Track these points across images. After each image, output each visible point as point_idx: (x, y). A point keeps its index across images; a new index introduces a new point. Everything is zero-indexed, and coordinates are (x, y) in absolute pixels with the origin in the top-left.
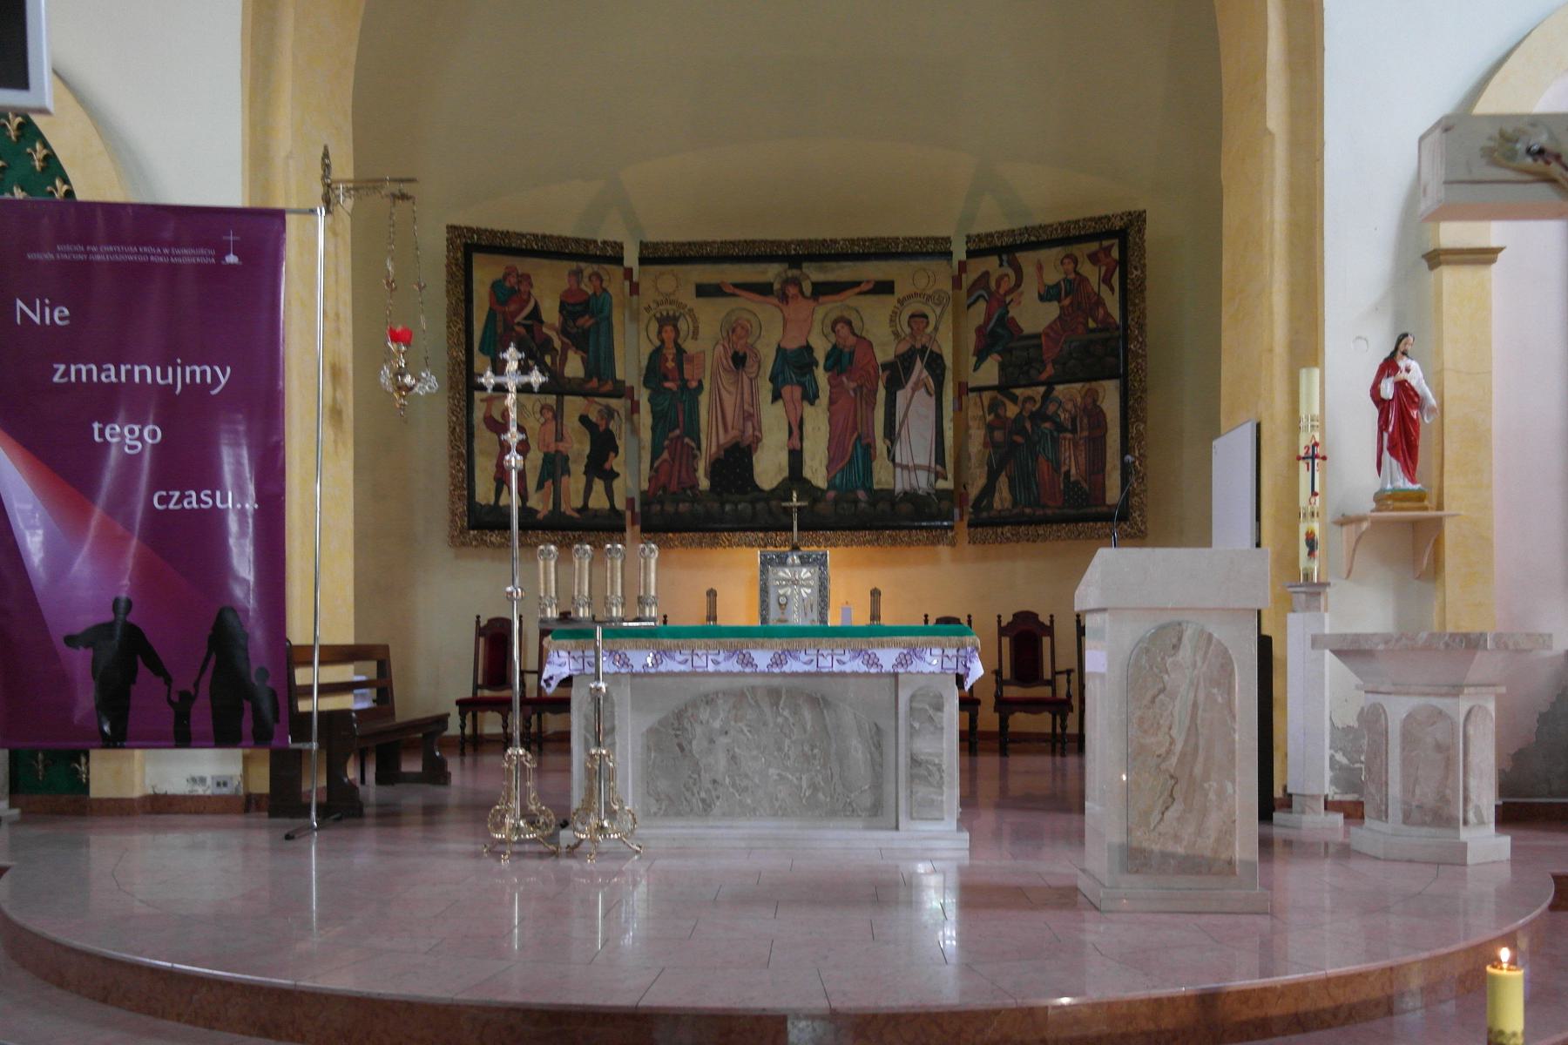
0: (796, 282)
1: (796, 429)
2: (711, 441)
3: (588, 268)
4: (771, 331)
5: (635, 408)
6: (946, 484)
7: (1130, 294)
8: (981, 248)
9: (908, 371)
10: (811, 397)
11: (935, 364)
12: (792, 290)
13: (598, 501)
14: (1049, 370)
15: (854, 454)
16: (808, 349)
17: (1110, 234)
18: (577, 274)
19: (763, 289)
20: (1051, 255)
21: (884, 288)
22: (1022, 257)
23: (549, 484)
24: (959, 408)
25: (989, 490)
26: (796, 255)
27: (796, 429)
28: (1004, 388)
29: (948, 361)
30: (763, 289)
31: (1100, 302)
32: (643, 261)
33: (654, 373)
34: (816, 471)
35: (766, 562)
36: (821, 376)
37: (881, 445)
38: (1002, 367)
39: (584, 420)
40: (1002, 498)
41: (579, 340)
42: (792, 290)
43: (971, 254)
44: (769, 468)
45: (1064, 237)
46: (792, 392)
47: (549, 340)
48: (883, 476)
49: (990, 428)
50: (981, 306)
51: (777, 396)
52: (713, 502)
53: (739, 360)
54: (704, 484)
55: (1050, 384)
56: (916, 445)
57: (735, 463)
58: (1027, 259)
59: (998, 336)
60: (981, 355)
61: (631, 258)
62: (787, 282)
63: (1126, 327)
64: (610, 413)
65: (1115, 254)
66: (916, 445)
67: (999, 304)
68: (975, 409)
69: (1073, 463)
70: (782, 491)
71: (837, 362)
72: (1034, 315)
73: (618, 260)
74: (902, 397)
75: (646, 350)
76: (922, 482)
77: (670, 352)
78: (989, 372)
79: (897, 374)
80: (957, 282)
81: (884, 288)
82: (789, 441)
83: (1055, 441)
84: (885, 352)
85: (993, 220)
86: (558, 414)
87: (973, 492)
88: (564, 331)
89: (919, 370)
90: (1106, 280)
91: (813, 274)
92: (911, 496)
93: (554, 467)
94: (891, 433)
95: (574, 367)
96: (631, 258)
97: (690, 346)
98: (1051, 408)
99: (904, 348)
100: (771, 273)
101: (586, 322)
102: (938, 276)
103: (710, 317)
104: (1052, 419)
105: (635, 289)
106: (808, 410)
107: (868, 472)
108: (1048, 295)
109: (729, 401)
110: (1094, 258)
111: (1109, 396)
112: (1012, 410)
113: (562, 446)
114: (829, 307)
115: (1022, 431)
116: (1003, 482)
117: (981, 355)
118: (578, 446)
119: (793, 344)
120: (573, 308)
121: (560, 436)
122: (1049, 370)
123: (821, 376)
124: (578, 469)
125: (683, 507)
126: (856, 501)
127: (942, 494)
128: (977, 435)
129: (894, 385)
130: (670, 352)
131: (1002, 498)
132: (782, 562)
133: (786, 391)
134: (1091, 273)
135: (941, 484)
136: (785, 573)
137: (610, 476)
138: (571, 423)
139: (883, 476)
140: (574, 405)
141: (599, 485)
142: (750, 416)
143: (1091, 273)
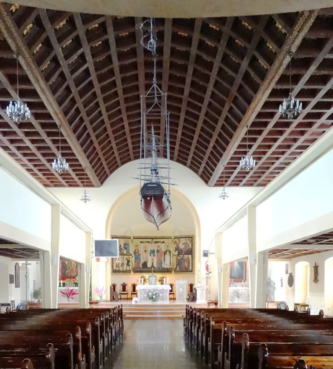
0: (153, 241)
1: (153, 260)
2: (142, 262)
3: (127, 239)
5: (132, 257)
7: (193, 245)
9: (166, 253)
10: (154, 256)
11: (170, 252)
12: (152, 242)
13: (128, 269)
14: (183, 253)
15: (160, 262)
16: (154, 250)
17: (191, 237)
19: (149, 242)
21: (163, 242)
22: (180, 239)
23: (122, 267)
24: (173, 257)
25: (176, 268)
27: (153, 260)
28: (178, 255)
30: (149, 242)
31: (189, 245)
33: (135, 253)
34: (155, 265)
36: (156, 253)
38: (178, 252)
39: (126, 259)
40: (178, 269)
41: (126, 249)
42: (152, 242)
44: (149, 265)
46: (152, 255)
47: (122, 249)
49: (176, 260)
50: (175, 245)
51: (150, 256)
52: (143, 268)
53: (146, 251)
54: (141, 267)
55: (183, 255)
57: (145, 264)
59: (177, 249)
60: (175, 251)
61: (132, 238)
62: (152, 241)
63: (192, 248)
64: (129, 257)
65: (191, 239)
68: (175, 257)
69: (186, 265)
70: (151, 268)
71: (158, 251)
72: (182, 246)
73: (130, 238)
74: (165, 256)
76: (168, 267)
77: (137, 250)
78: (176, 253)
79: (165, 253)
80: (172, 242)
81: (163, 242)
82: (152, 261)
83: (184, 262)
84: (164, 250)
85: (177, 234)
86: (123, 258)
87: (174, 268)
89: (168, 252)
90: (190, 243)
91: (155, 240)
92: (167, 268)
93: (123, 264)
94: (164, 260)
96: (132, 238)
97: (139, 249)
98: (184, 258)
99: (166, 250)
101: (126, 246)
102: (170, 240)
103: (142, 245)
104: (184, 259)
105: (132, 242)
107: (162, 266)
108: (183, 244)
109: (144, 256)
110: (188, 240)
112: (179, 258)
115: (180, 261)
116: (178, 267)
118: (126, 262)
119: (152, 249)
120: (125, 245)
121: (123, 261)
122: (183, 253)
123: (156, 253)
125: (139, 269)
126: (160, 269)
127: (171, 268)
128: (175, 261)
129: (165, 254)
130: (137, 250)
131: (178, 269)
132: (151, 276)
133: (151, 255)
135: (171, 267)
136: (151, 278)
137: (129, 265)
139: (163, 266)
140: (125, 257)
141: (128, 266)
143: (188, 242)
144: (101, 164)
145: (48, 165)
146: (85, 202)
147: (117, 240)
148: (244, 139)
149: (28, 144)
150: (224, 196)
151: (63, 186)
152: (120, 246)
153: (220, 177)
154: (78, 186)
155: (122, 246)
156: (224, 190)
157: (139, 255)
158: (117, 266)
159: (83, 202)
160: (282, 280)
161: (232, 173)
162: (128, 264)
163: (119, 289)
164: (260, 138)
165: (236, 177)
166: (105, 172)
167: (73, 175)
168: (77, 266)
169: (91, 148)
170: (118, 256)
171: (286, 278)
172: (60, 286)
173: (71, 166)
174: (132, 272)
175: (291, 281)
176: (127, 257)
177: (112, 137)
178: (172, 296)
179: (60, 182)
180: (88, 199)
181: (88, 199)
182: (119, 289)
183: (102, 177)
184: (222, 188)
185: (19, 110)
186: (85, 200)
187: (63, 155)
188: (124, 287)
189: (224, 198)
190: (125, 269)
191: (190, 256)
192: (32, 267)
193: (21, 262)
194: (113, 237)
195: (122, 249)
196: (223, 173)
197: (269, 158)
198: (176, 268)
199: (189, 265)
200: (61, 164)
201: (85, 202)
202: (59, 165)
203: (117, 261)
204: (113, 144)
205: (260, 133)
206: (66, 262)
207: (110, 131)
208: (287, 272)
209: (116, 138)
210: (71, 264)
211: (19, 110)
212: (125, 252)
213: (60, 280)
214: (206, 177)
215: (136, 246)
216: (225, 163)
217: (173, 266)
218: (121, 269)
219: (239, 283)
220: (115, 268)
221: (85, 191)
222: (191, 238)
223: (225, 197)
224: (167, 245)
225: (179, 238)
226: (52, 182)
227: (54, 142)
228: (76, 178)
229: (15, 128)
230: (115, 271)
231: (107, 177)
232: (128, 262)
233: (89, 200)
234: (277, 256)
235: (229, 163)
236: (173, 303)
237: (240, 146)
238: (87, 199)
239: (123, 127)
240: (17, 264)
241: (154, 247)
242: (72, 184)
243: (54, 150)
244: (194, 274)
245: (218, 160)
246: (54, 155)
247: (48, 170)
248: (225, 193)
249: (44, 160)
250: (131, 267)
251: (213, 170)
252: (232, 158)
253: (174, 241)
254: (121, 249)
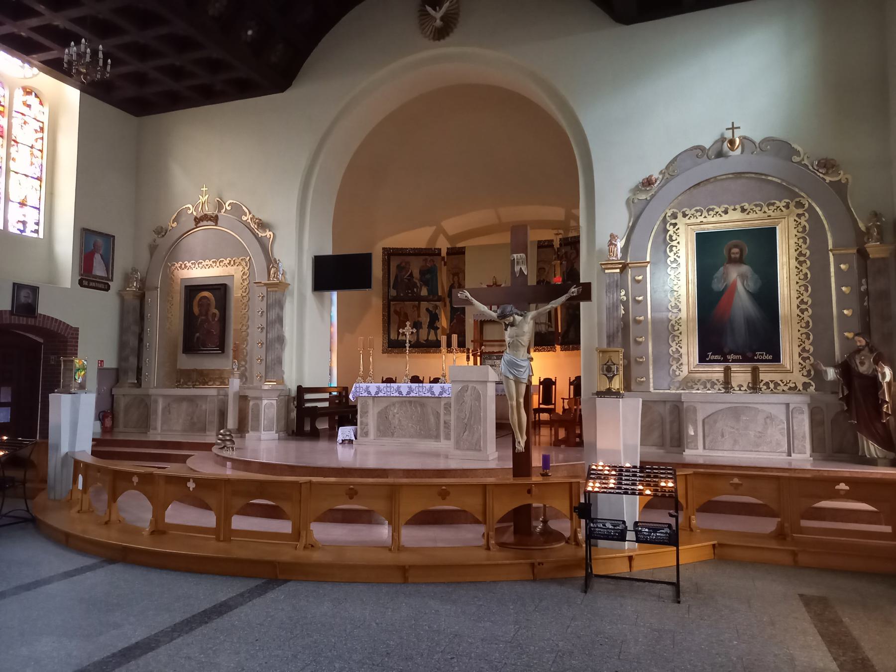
5: (445, 305)
6: (553, 329)
13: (432, 337)
18: (426, 260)
32: (448, 254)
39: (427, 310)
41: (426, 283)
64: (436, 307)
73: (439, 254)
86: (418, 307)
88: (421, 280)
95: (424, 292)
101: (428, 276)
113: (420, 319)
118: (425, 319)
120: (422, 273)
124: (425, 326)
135: (550, 329)
140: (424, 305)
141: (432, 332)
195: (415, 285)
212: (424, 292)
215: (454, 275)
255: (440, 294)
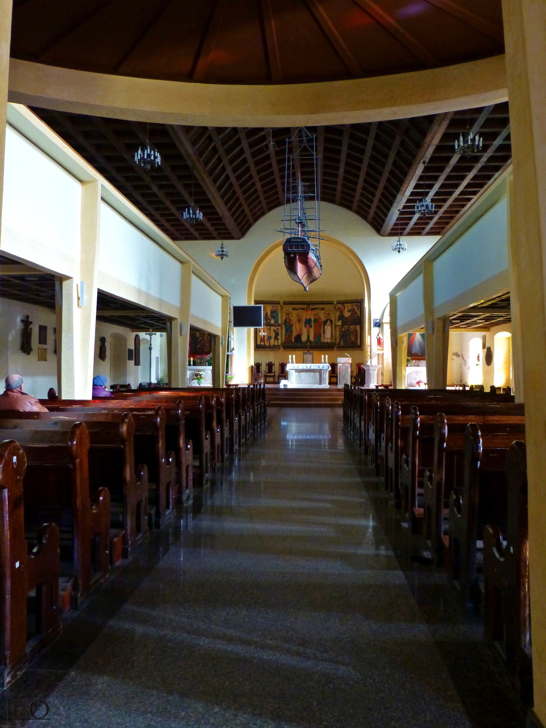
0: (309, 308)
1: (308, 332)
2: (295, 334)
4: (305, 315)
5: (282, 328)
8: (339, 302)
10: (311, 326)
11: (331, 322)
13: (276, 344)
15: (318, 335)
16: (310, 319)
19: (303, 309)
20: (349, 305)
24: (335, 328)
25: (340, 342)
26: (309, 304)
27: (308, 332)
28: (342, 326)
29: (333, 320)
30: (303, 309)
34: (312, 339)
35: (304, 354)
36: (313, 323)
37: (322, 335)
38: (342, 322)
39: (274, 330)
40: (342, 344)
41: (273, 317)
43: (337, 303)
44: (304, 338)
45: (352, 302)
48: (322, 340)
49: (340, 332)
51: (305, 326)
52: (294, 344)
54: (293, 341)
55: (349, 325)
56: (328, 335)
57: (299, 337)
58: (346, 305)
59: (341, 317)
60: (339, 320)
61: (282, 303)
62: (307, 308)
64: (278, 329)
66: (328, 335)
67: (342, 312)
68: (338, 329)
69: (353, 338)
70: (306, 342)
71: (316, 321)
72: (347, 314)
74: (326, 327)
75: (284, 319)
76: (329, 341)
78: (340, 323)
79: (325, 323)
80: (335, 308)
81: (323, 309)
84: (323, 319)
86: (270, 330)
90: (358, 309)
91: (312, 306)
92: (327, 343)
93: (269, 338)
94: (324, 333)
95: (272, 322)
96: (282, 303)
97: (291, 318)
99: (326, 319)
100: (305, 306)
101: (274, 314)
102: (332, 307)
103: (295, 313)
105: (282, 309)
106: (310, 329)
107: (320, 339)
108: (349, 311)
110: (356, 306)
111: (358, 328)
112: (343, 329)
114: (315, 312)
116: (342, 341)
117: (339, 320)
118: (273, 335)
119: (308, 318)
120: (273, 312)
122: (349, 323)
123: (313, 323)
124: (273, 338)
127: (333, 343)
128: (338, 333)
131: (342, 344)
132: (306, 354)
134: (356, 308)
137: (278, 339)
138: (272, 331)
139: (322, 340)
140: (272, 328)
141: (276, 341)
142: (301, 330)
143: (356, 308)
144: (243, 211)
145: (178, 215)
146: (222, 258)
147: (262, 306)
148: (421, 178)
149: (155, 189)
150: (399, 249)
151: (195, 238)
152: (267, 313)
153: (395, 224)
154: (213, 238)
155: (269, 313)
156: (399, 241)
157: (291, 326)
158: (263, 339)
159: (219, 258)
160: (478, 357)
161: (410, 219)
162: (276, 338)
163: (264, 368)
164: (443, 177)
165: (416, 224)
166: (248, 220)
167: (208, 225)
168: (210, 340)
169: (231, 192)
170: (263, 327)
171: (482, 353)
172: (190, 365)
173: (204, 214)
174: (282, 349)
175: (489, 358)
176: (275, 328)
177: (256, 178)
178: (334, 380)
179: (192, 234)
180: (226, 255)
181: (226, 255)
182: (264, 368)
183: (243, 229)
184: (397, 238)
185: (149, 156)
186: (222, 255)
187: (196, 201)
188: (270, 366)
189: (399, 251)
190: (272, 344)
191: (358, 328)
192: (158, 340)
193: (143, 335)
194: (256, 302)
195: (268, 318)
196: (397, 220)
197: (456, 200)
198: (340, 342)
199: (356, 339)
200: (194, 213)
201: (222, 258)
202: (191, 215)
203: (262, 334)
204: (258, 185)
205: (442, 169)
206: (198, 335)
207: (253, 170)
208: (484, 347)
209: (261, 179)
210: (203, 337)
211: (149, 156)
212: (272, 322)
213: (189, 357)
214: (378, 226)
216: (400, 207)
217: (336, 340)
218: (267, 344)
219: (421, 361)
220: (259, 343)
221: (222, 245)
222: (359, 303)
223: (401, 250)
224: (328, 312)
225: (343, 303)
226: (182, 234)
227: (186, 186)
228: (211, 229)
229: (147, 180)
230: (258, 347)
231: (250, 226)
232: (277, 334)
233: (226, 256)
234: (469, 325)
235: (405, 207)
236: (333, 387)
237: (417, 186)
238: (224, 255)
239: (270, 166)
240: (137, 337)
241: (310, 315)
242: (206, 236)
243: (186, 196)
244: (362, 350)
245: (391, 204)
246: (185, 202)
247: (178, 220)
248: (400, 245)
249: (173, 210)
250: (279, 341)
251: (386, 216)
252: (408, 201)
253: (337, 307)
254: (266, 318)
255: (280, 323)
